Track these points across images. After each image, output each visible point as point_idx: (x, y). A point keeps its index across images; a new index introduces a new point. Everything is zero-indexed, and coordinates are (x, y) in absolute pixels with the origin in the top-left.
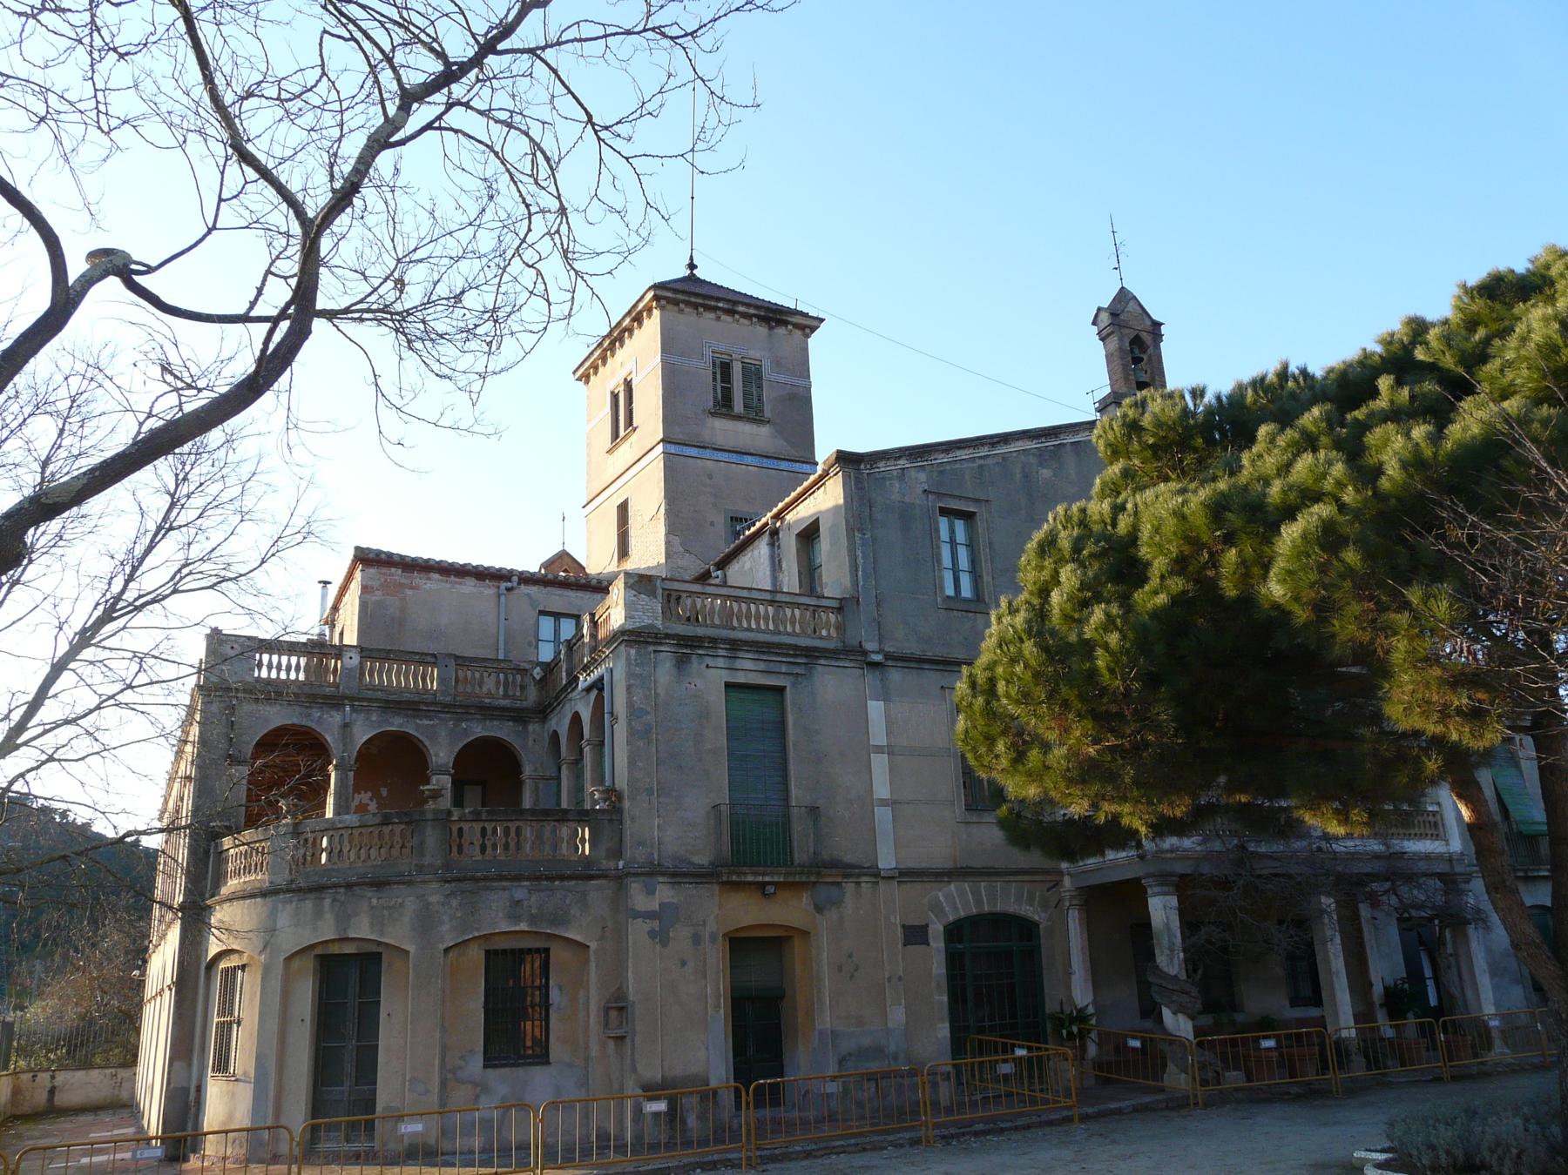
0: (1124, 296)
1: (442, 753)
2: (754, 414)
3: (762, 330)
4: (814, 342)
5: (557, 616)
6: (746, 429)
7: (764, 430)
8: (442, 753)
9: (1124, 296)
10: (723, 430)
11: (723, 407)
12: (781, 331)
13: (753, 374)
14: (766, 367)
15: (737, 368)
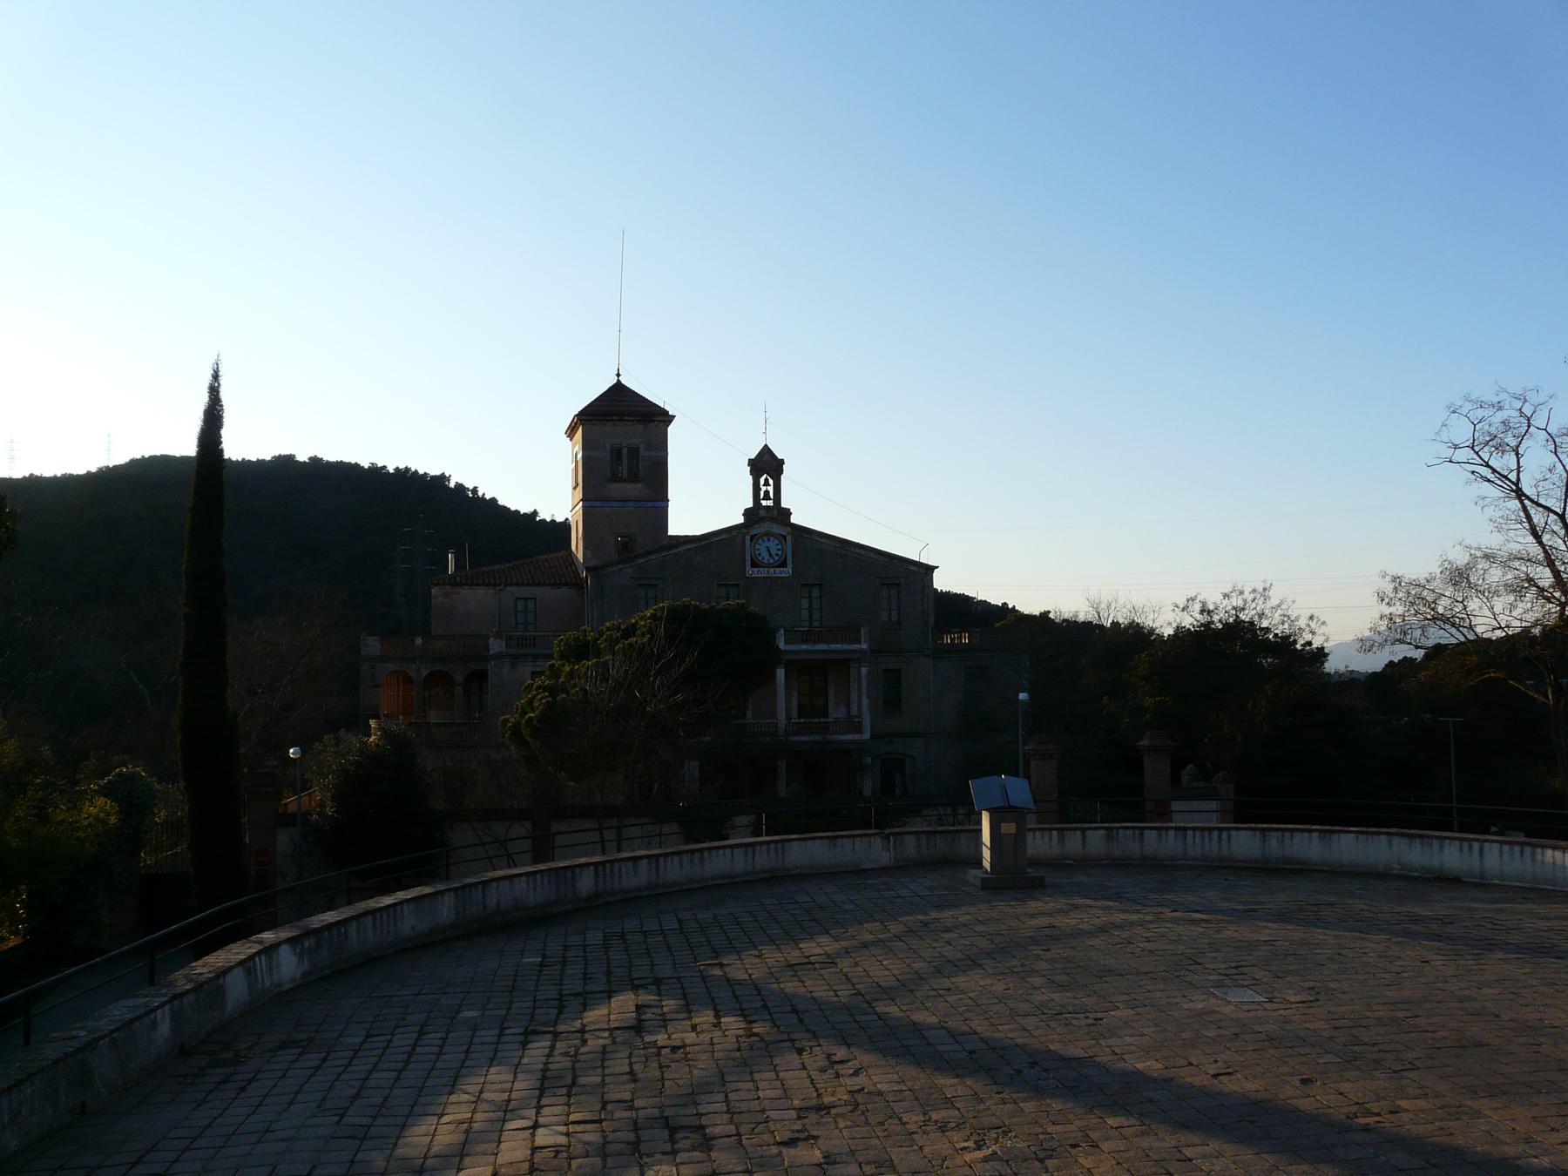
0: (766, 451)
1: (459, 678)
2: (634, 478)
3: (640, 427)
4: (673, 431)
5: (526, 599)
6: (629, 486)
7: (639, 486)
8: (459, 678)
9: (766, 451)
10: (616, 489)
11: (615, 478)
12: (652, 425)
13: (634, 452)
14: (642, 447)
15: (625, 451)
